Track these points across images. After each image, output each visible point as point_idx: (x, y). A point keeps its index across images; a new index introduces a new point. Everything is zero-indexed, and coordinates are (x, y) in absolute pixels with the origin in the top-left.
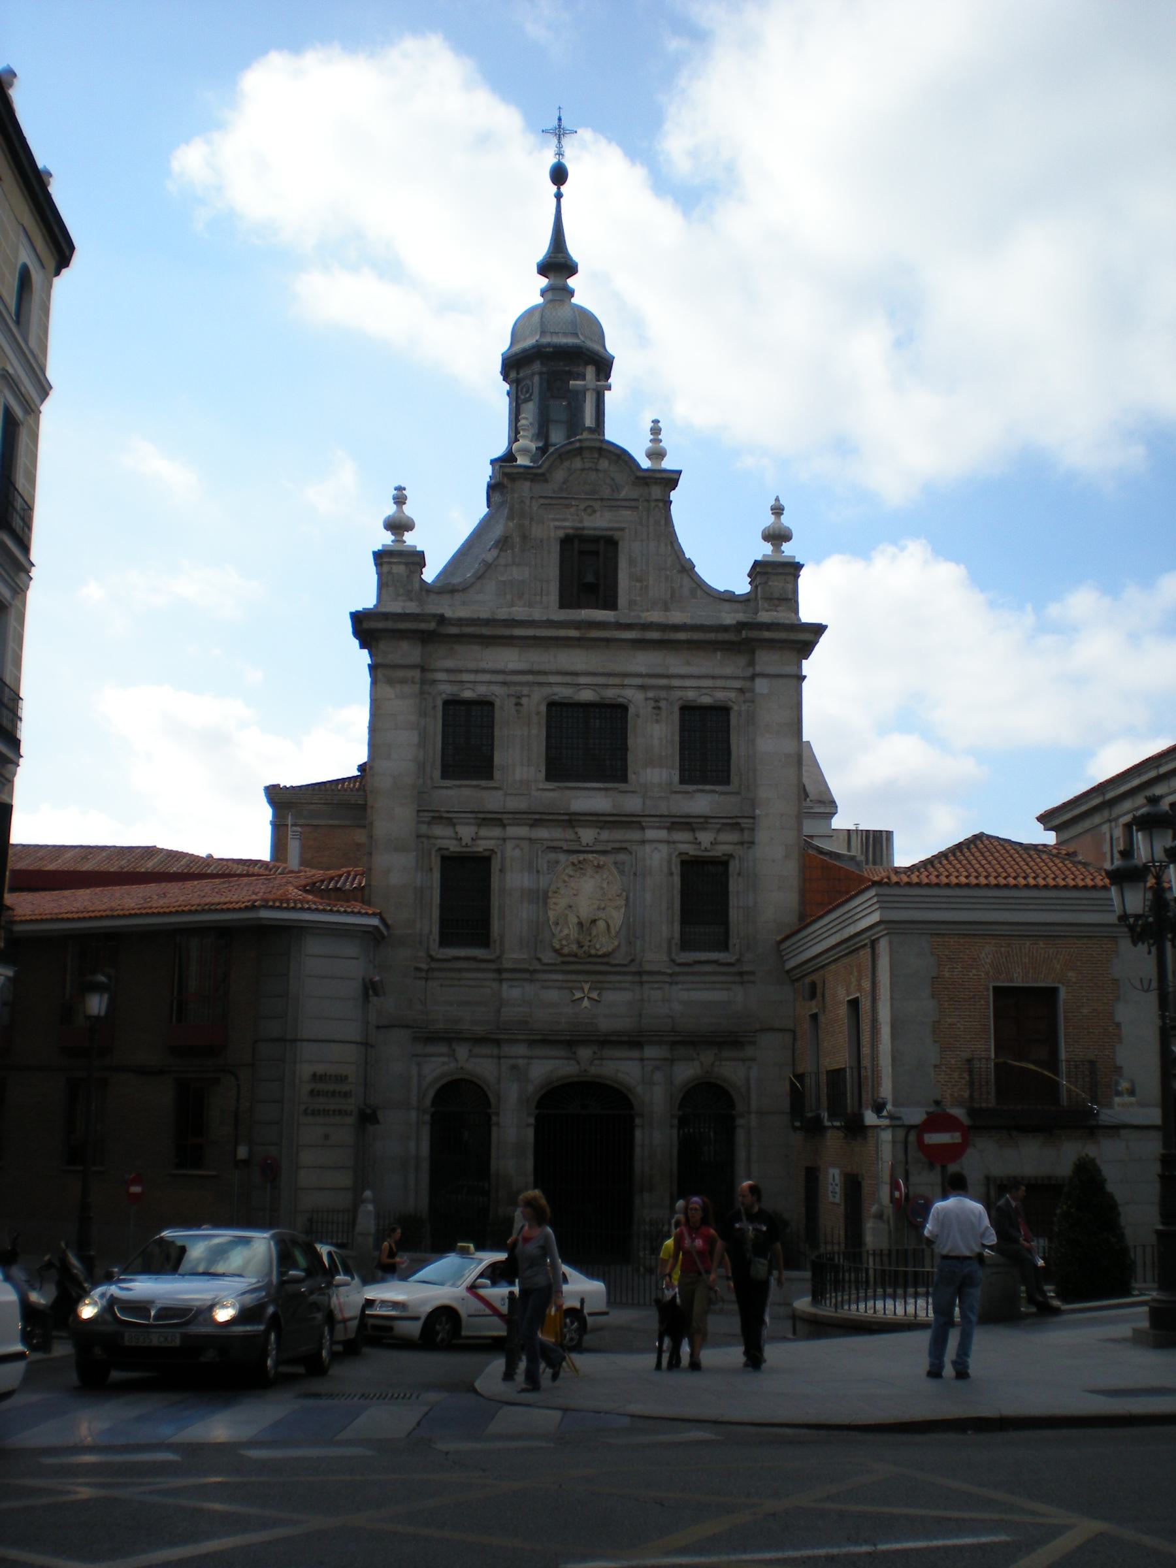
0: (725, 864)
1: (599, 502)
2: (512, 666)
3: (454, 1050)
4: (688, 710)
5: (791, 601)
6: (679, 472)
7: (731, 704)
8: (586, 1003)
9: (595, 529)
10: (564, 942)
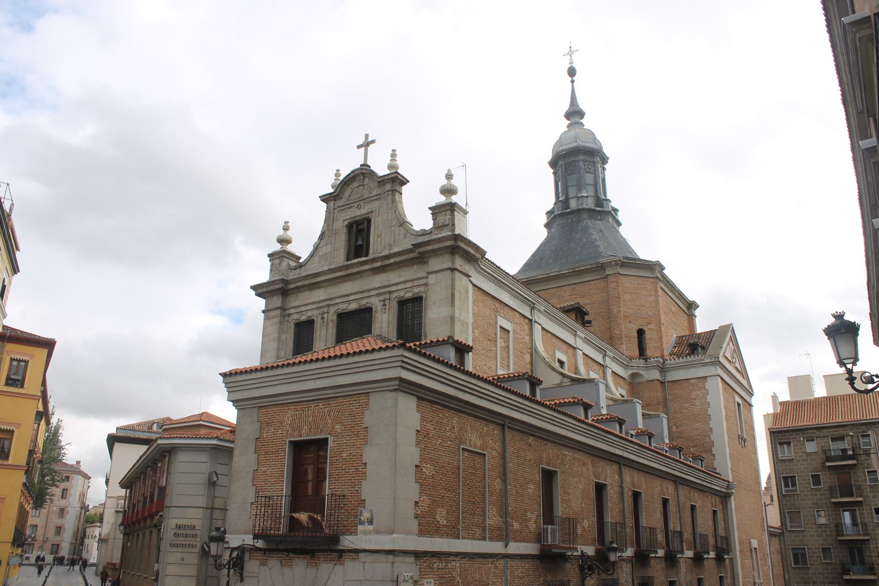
1: (363, 201)
2: (321, 298)
4: (402, 303)
7: (421, 294)
9: (360, 216)
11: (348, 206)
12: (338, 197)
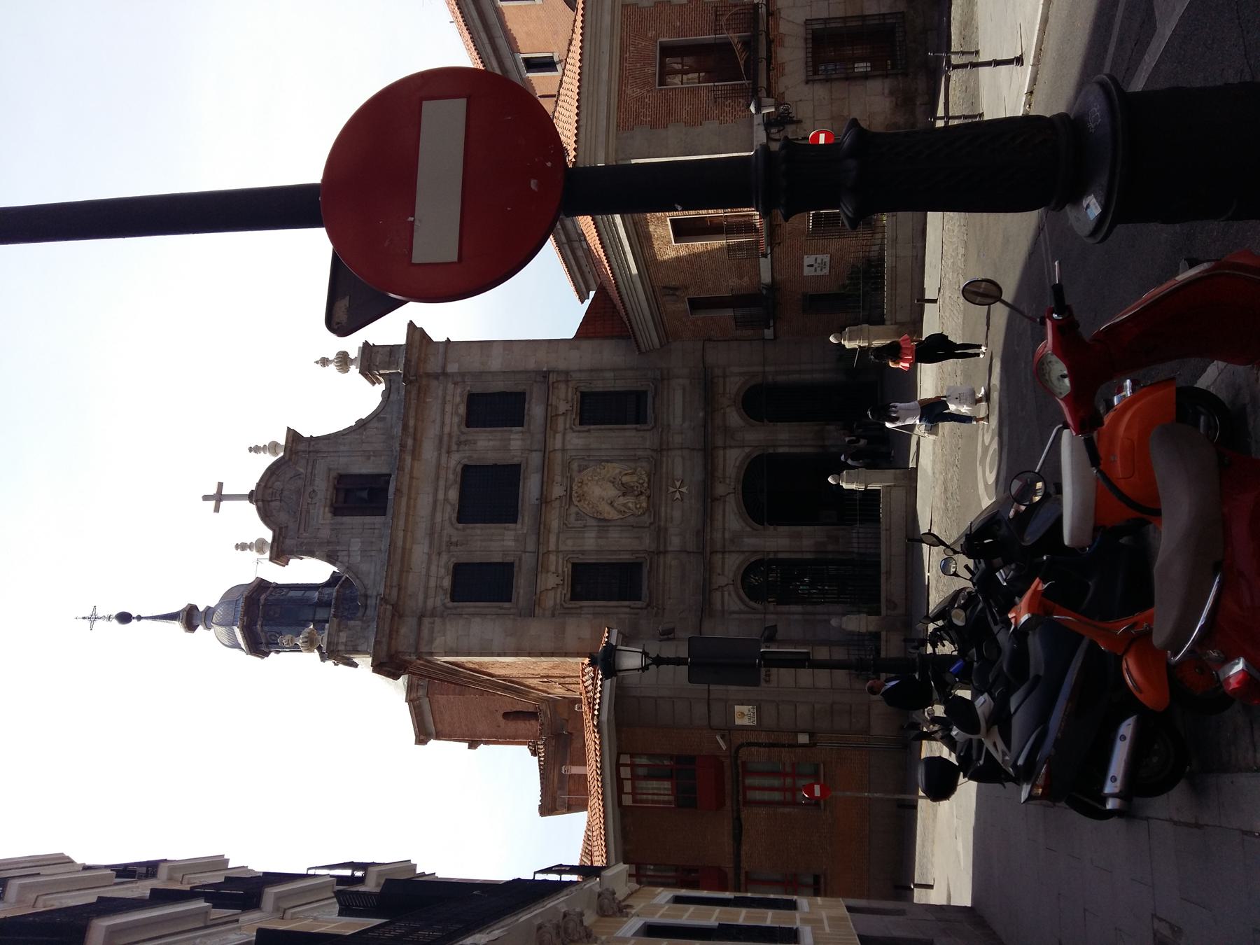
0: (583, 395)
2: (426, 550)
3: (719, 587)
5: (393, 349)
6: (289, 429)
7: (466, 393)
8: (683, 490)
10: (638, 506)
11: (303, 514)
12: (283, 530)
